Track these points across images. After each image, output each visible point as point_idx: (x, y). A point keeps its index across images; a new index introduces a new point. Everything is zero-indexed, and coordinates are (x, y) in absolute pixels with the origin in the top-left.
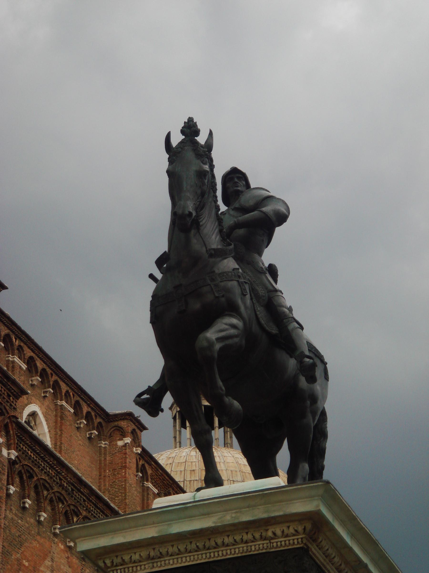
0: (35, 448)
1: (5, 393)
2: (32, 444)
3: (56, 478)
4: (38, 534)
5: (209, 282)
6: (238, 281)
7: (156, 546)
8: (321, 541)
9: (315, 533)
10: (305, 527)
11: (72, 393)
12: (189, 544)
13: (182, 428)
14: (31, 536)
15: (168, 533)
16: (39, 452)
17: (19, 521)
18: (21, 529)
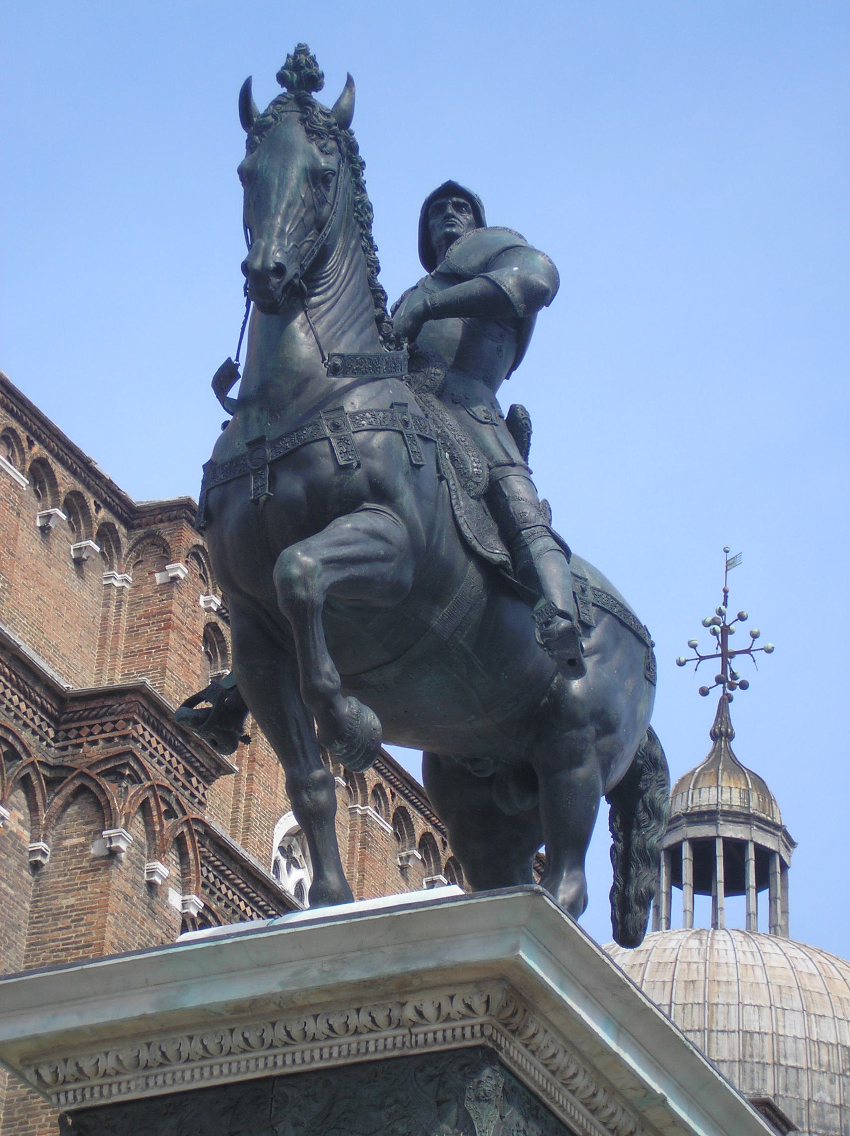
0: (254, 895)
1: (180, 767)
2: (248, 887)
5: (328, 432)
7: (155, 1039)
8: (534, 1035)
9: (514, 1014)
10: (488, 996)
11: (391, 791)
12: (228, 1033)
13: (673, 887)
15: (179, 1006)
16: (265, 905)
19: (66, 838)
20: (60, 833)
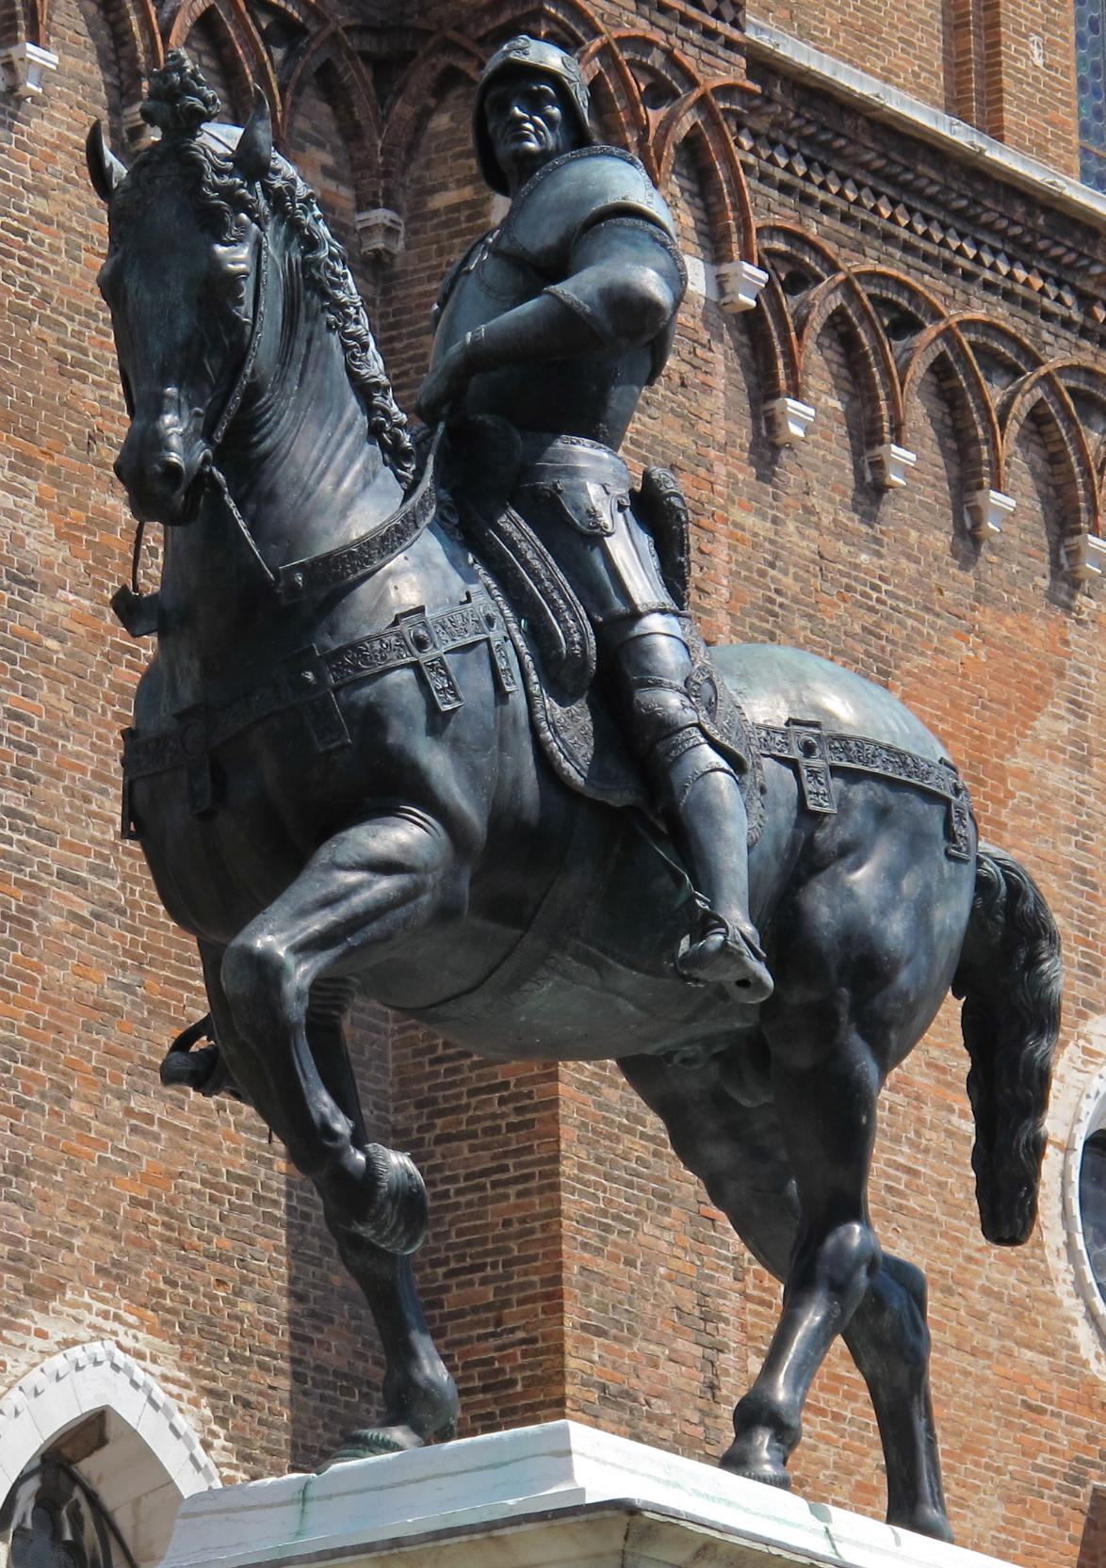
0: (910, 176)
2: (892, 162)
3: (1059, 299)
4: (977, 600)
6: (415, 666)
14: (938, 615)
16: (939, 192)
17: (864, 558)
18: (875, 595)
19: (433, 191)
20: (419, 180)
